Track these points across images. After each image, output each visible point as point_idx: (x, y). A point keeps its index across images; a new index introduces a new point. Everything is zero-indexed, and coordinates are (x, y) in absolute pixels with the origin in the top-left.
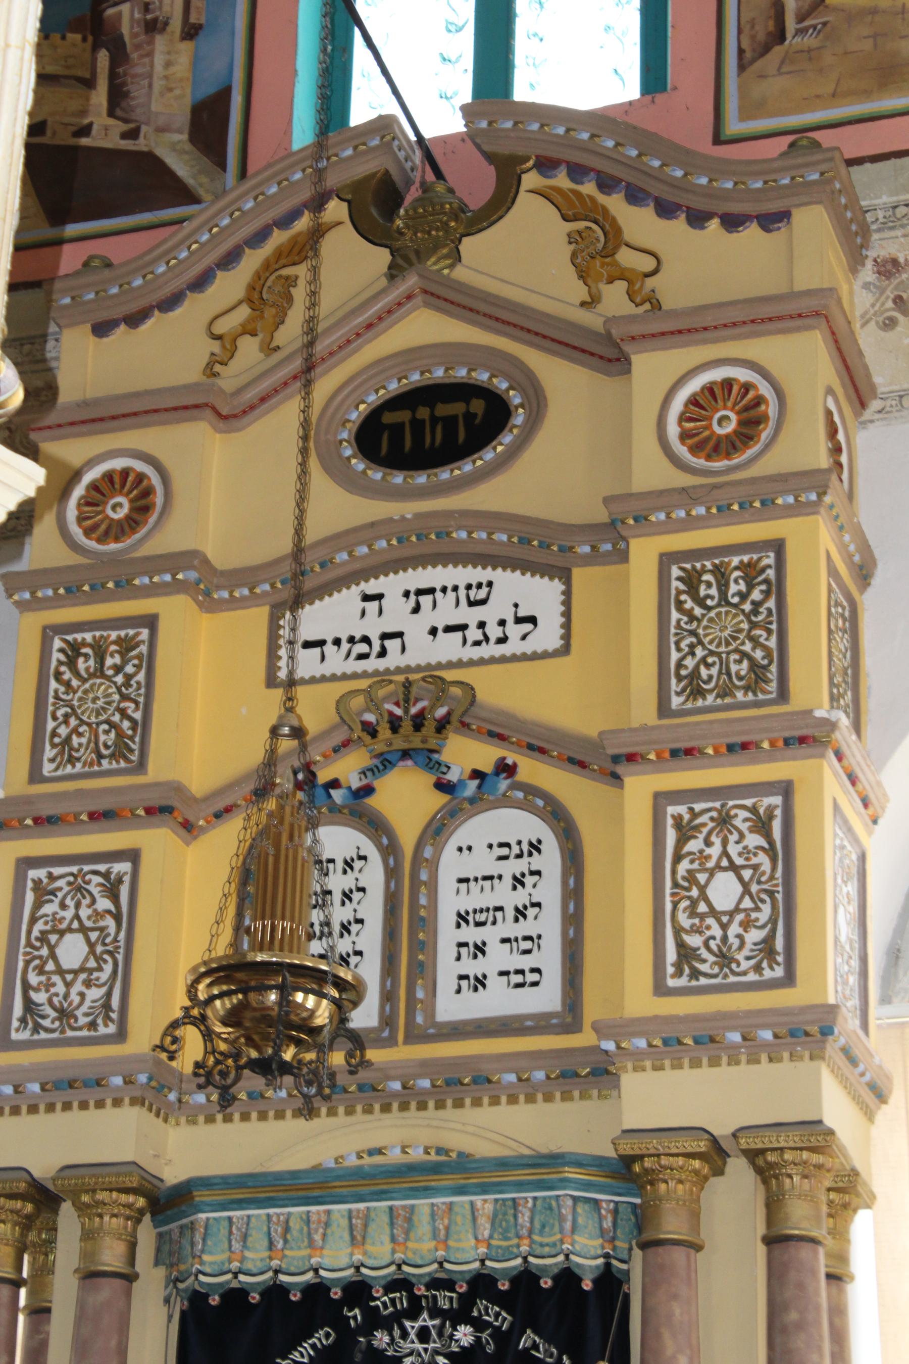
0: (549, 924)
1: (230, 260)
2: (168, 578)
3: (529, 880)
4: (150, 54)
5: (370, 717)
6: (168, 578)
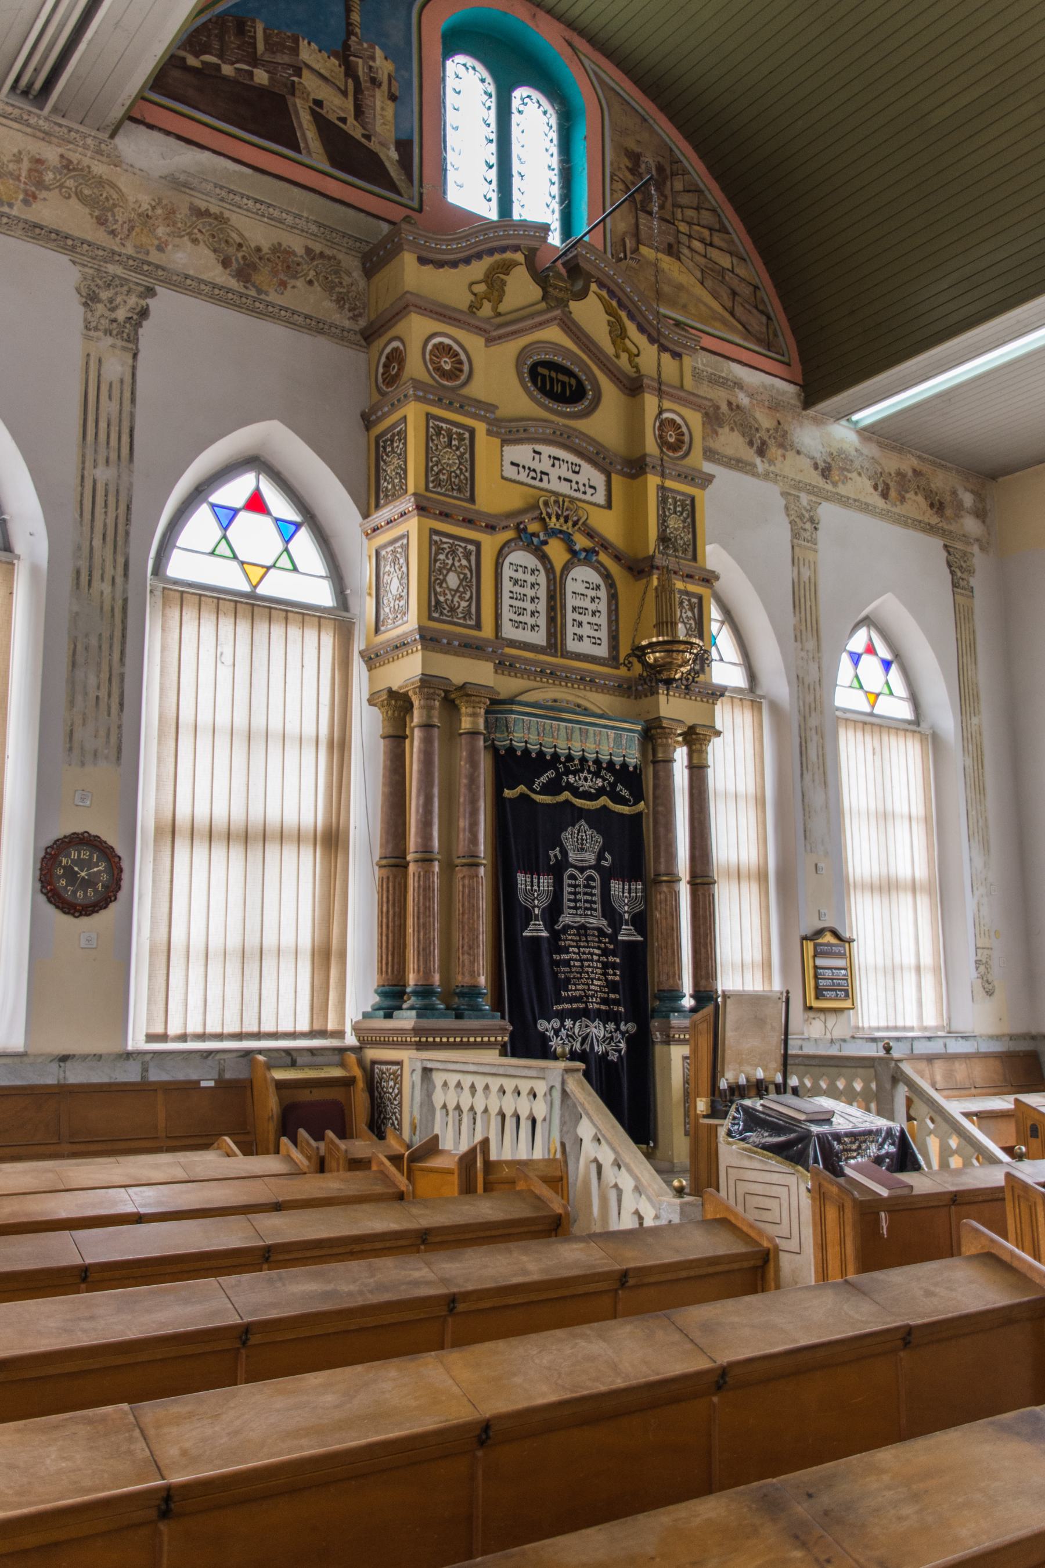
0: (603, 620)
1: (479, 256)
2: (483, 413)
3: (597, 601)
4: (374, 96)
5: (550, 511)
6: (483, 413)
